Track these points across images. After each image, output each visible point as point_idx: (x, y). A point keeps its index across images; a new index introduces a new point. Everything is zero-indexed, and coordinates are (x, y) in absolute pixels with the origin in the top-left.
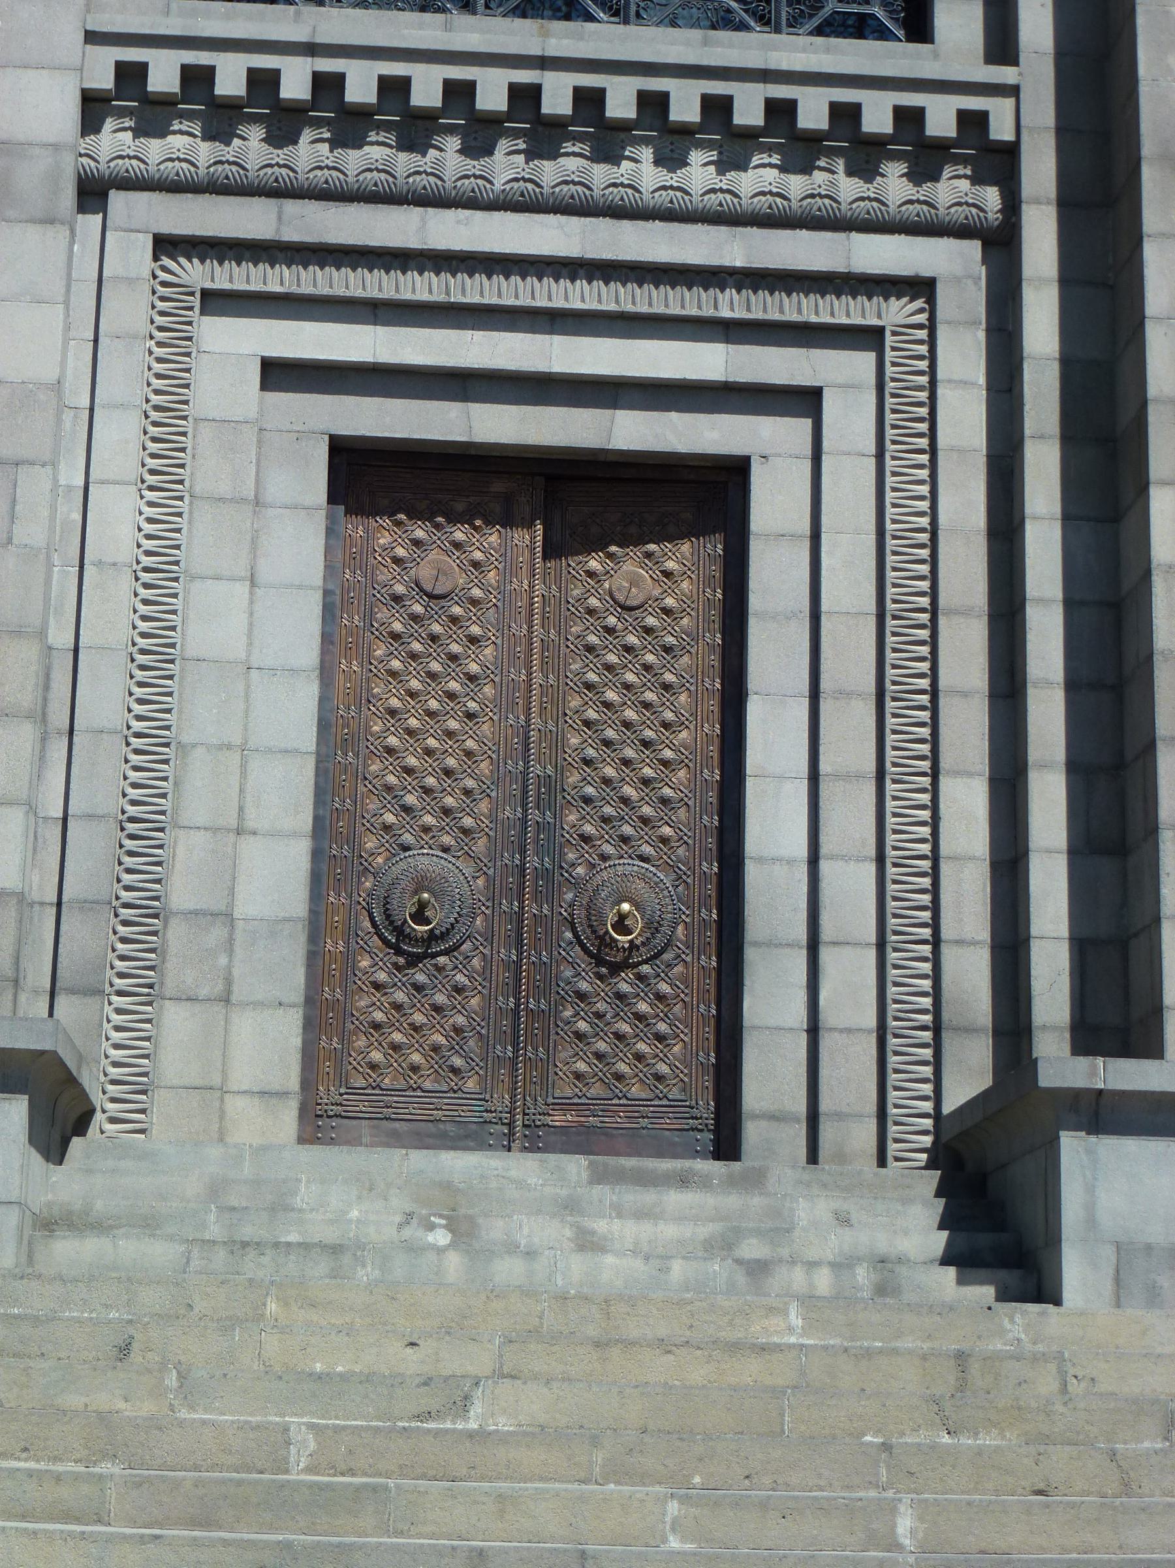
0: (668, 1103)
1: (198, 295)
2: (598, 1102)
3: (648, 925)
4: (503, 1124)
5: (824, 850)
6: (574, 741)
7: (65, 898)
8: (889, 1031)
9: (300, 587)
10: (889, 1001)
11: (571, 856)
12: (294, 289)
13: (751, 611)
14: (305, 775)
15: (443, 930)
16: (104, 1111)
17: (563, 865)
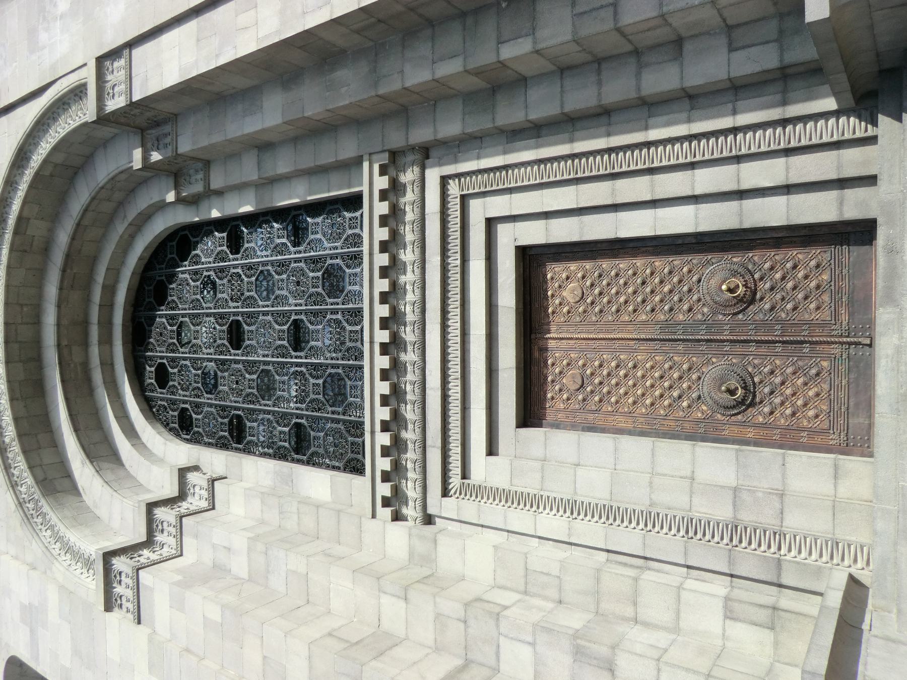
0: (833, 260)
1: (464, 481)
2: (833, 297)
3: (734, 276)
4: (849, 348)
5: (689, 193)
6: (644, 317)
7: (728, 572)
8: (787, 147)
9: (579, 444)
10: (769, 149)
11: (700, 317)
12: (459, 442)
13: (579, 240)
14: (665, 446)
15: (740, 379)
16: (850, 566)
17: (704, 319)
